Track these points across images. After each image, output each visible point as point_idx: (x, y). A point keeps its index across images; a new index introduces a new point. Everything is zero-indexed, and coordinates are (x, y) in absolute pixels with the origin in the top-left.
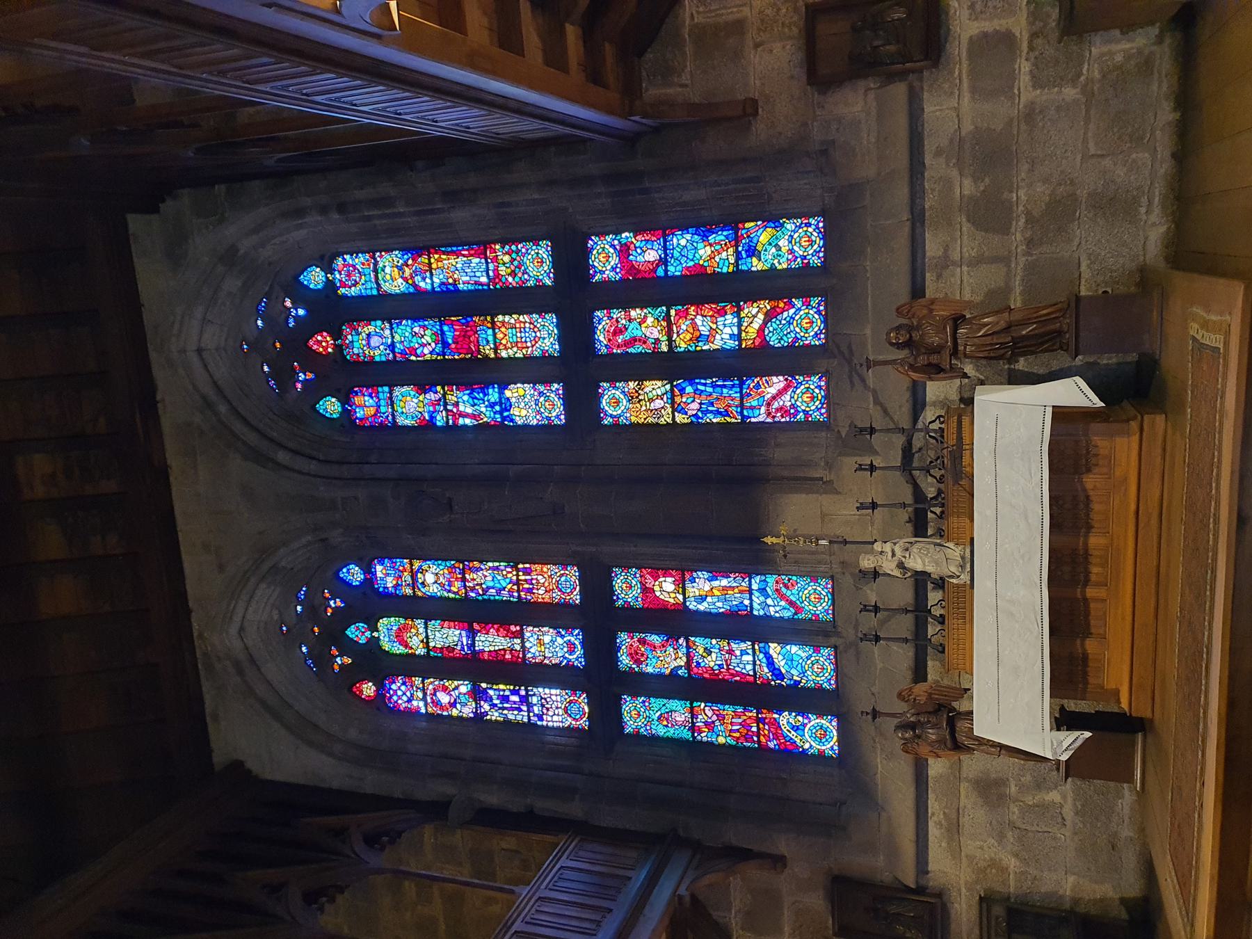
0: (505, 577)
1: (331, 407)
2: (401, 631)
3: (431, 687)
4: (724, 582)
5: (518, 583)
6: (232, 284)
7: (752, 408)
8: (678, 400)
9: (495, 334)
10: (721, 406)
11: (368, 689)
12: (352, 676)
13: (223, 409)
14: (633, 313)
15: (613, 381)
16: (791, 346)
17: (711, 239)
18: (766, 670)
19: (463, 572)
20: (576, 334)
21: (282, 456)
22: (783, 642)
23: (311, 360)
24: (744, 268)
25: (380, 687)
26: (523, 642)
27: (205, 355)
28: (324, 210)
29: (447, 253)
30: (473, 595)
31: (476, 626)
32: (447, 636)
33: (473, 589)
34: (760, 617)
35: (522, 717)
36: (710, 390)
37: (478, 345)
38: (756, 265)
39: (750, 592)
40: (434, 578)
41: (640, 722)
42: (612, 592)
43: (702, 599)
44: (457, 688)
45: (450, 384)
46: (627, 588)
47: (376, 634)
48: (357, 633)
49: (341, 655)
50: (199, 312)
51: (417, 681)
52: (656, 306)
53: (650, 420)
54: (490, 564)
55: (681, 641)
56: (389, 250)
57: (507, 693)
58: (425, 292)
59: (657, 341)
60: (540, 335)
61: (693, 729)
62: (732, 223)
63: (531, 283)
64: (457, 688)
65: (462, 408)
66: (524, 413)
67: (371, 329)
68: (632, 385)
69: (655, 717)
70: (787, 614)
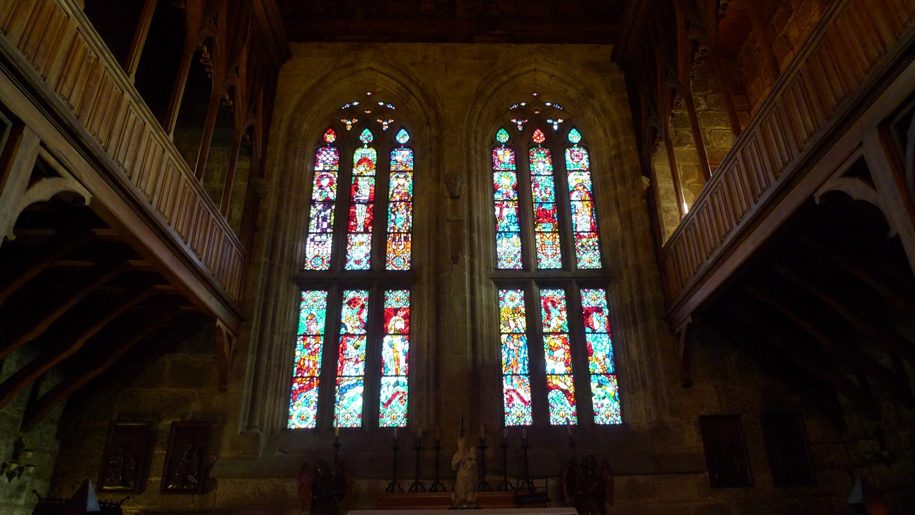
0: (403, 225)
1: (503, 136)
2: (369, 162)
3: (332, 175)
4: (403, 359)
5: (399, 233)
6: (572, 93)
7: (512, 381)
8: (515, 336)
10: (512, 362)
11: (331, 138)
12: (339, 129)
13: (505, 78)
14: (564, 314)
15: (525, 298)
16: (548, 405)
17: (608, 360)
18: (346, 384)
19: (404, 201)
20: (550, 280)
21: (480, 106)
22: (365, 395)
23: (529, 130)
24: (592, 377)
25: (332, 145)
26: (361, 233)
27: (533, 73)
28: (617, 146)
29: (592, 210)
30: (391, 205)
31: (371, 206)
32: (365, 188)
33: (395, 205)
34: (380, 382)
35: (313, 228)
36: (522, 356)
37: (542, 222)
38: (594, 385)
39: (397, 375)
40: (401, 184)
41: (310, 302)
42: (395, 289)
43: (391, 345)
44: (332, 191)
45: (518, 204)
46: (397, 299)
47: (366, 146)
48: (366, 135)
49: (352, 124)
50: (556, 73)
51: (336, 168)
52: (569, 326)
53: (502, 319)
54: (411, 217)
55: (364, 331)
56: (592, 179)
57: (329, 221)
58: (569, 196)
59: (549, 326)
60: (549, 258)
61: (305, 336)
62: (618, 372)
63: (578, 256)
64: (332, 191)
66: (504, 245)
67: (548, 164)
68: (523, 310)
69: (313, 312)
70: (383, 399)
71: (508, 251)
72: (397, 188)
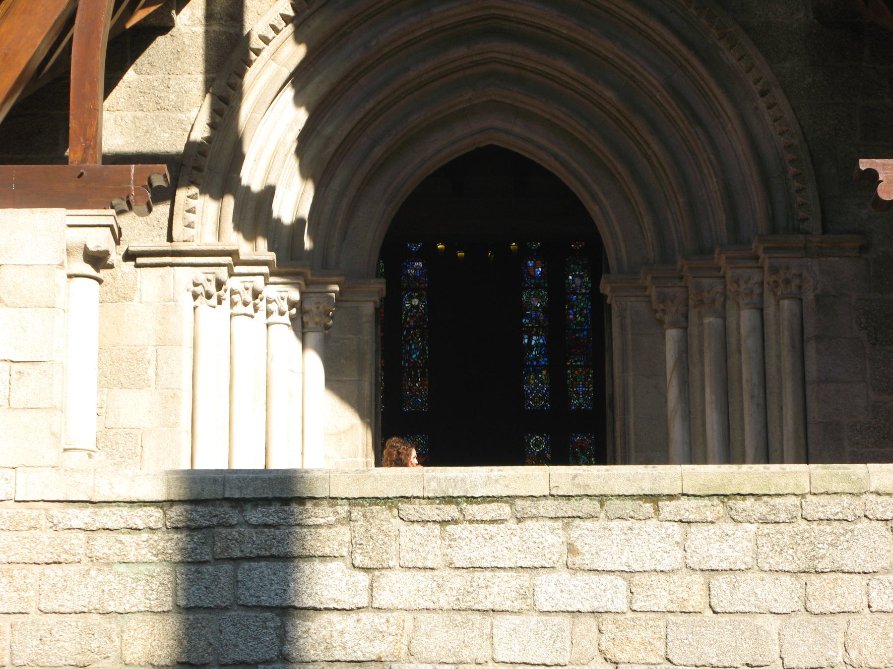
0: (418, 357)
9: (581, 366)
65: (534, 338)
68: (548, 456)
71: (536, 386)
72: (410, 310)
